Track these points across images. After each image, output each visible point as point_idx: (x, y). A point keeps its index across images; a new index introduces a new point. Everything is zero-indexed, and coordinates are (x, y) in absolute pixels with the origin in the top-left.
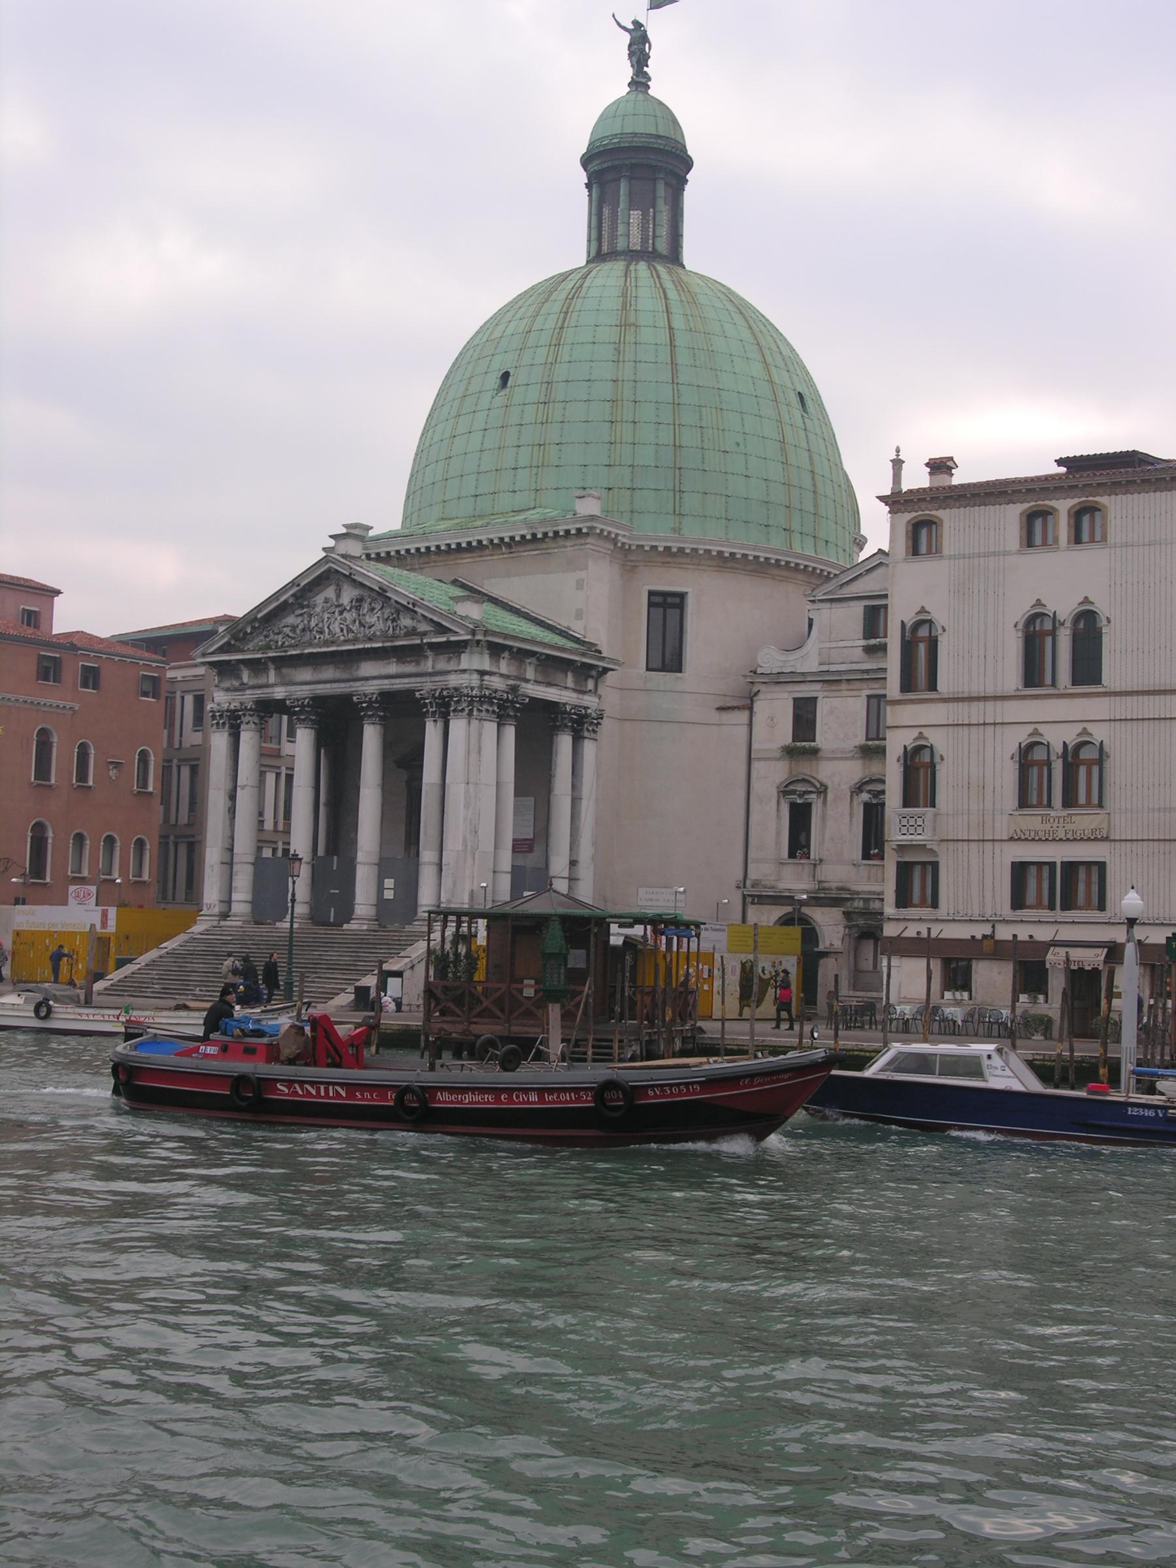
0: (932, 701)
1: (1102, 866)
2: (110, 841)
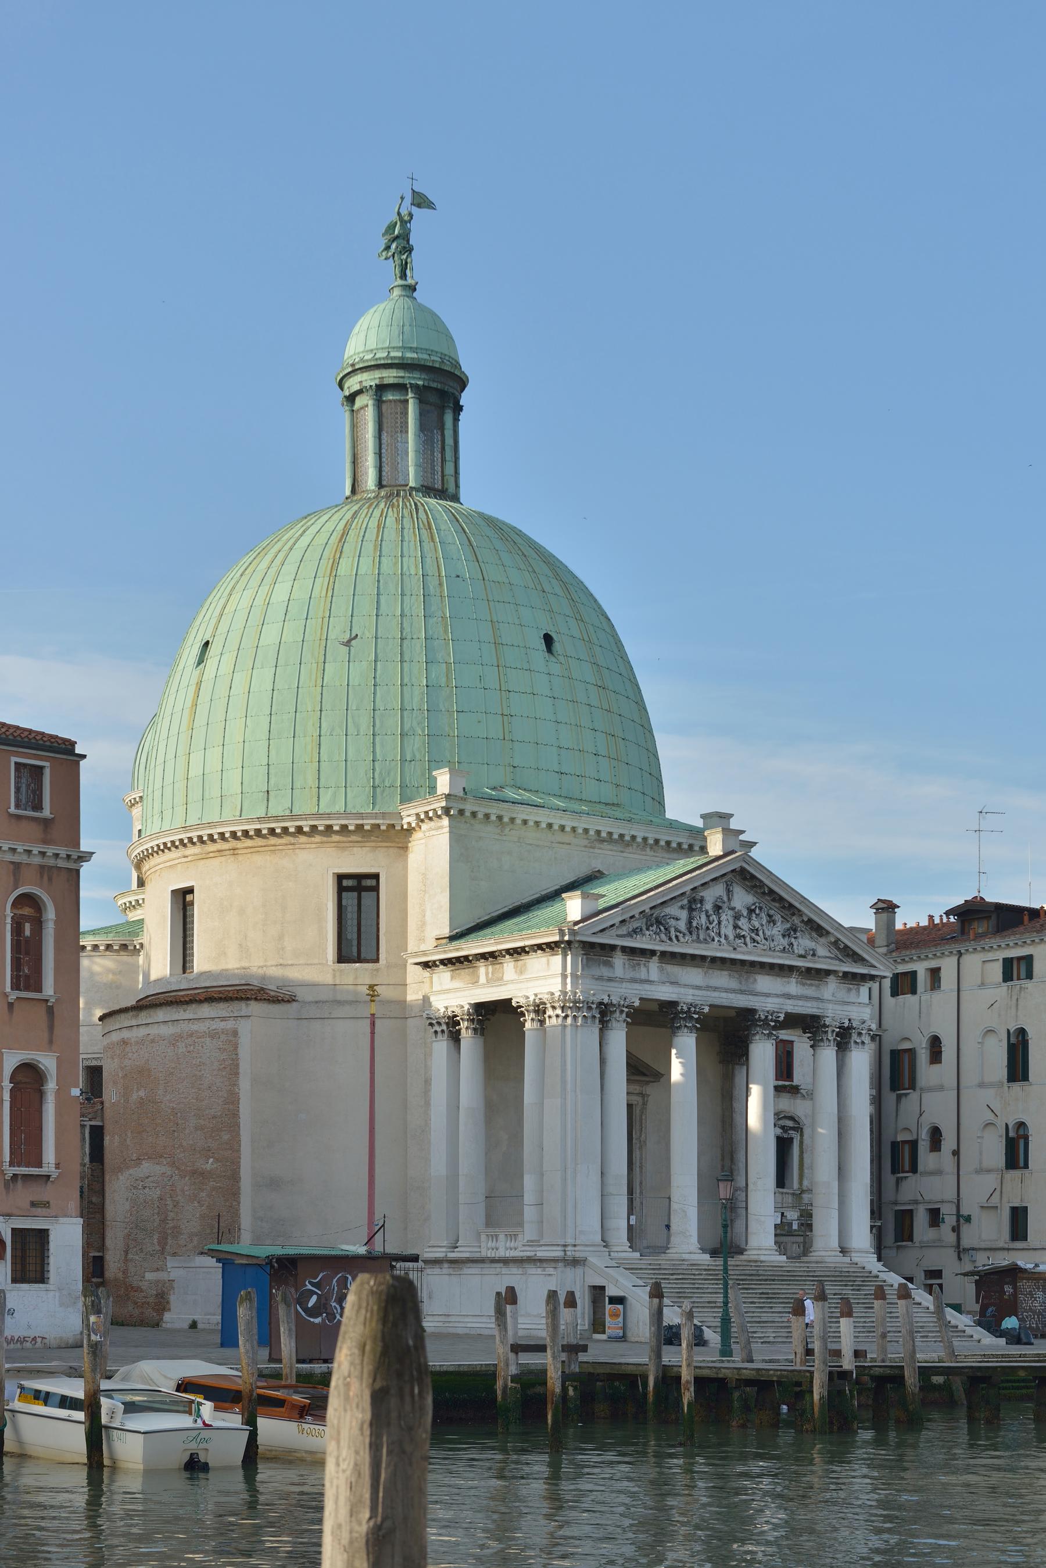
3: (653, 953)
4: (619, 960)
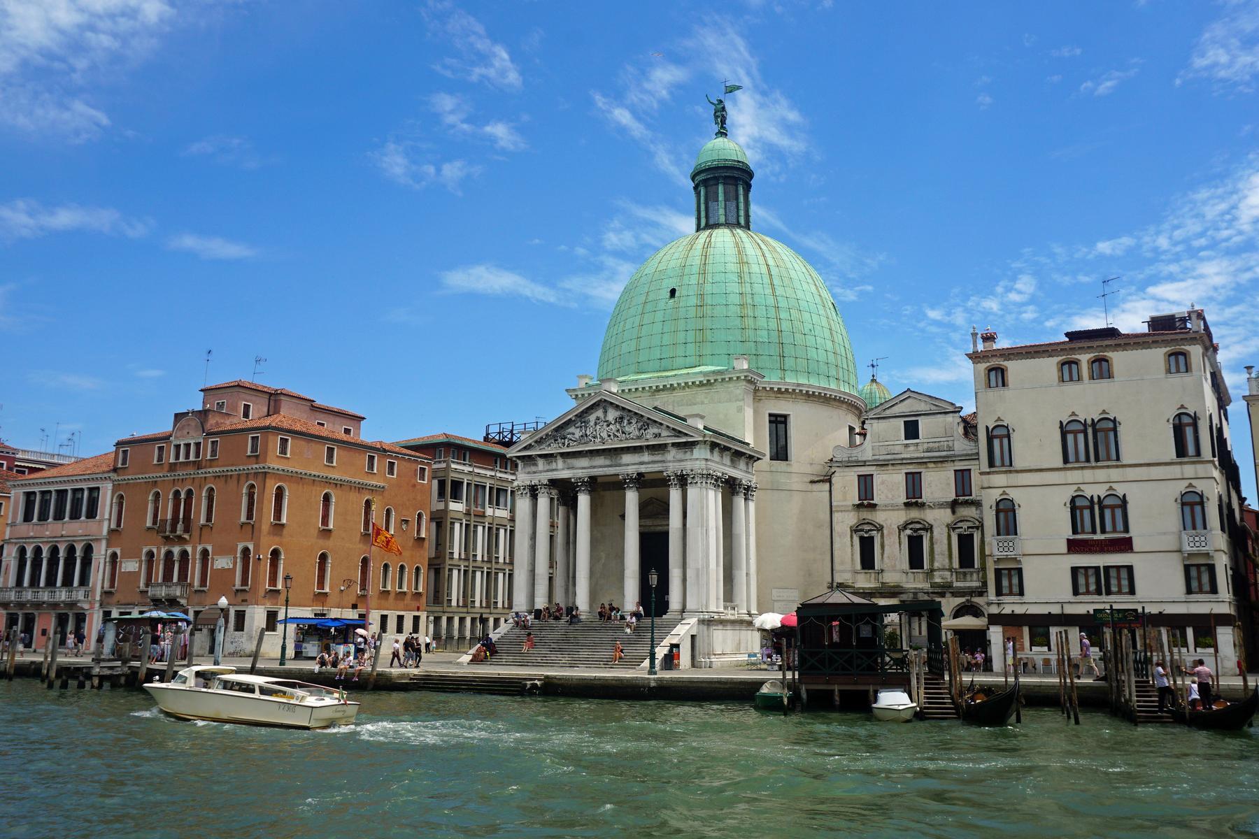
0: (1010, 472)
1: (1130, 569)
2: (402, 567)
3: (551, 455)
4: (541, 462)
